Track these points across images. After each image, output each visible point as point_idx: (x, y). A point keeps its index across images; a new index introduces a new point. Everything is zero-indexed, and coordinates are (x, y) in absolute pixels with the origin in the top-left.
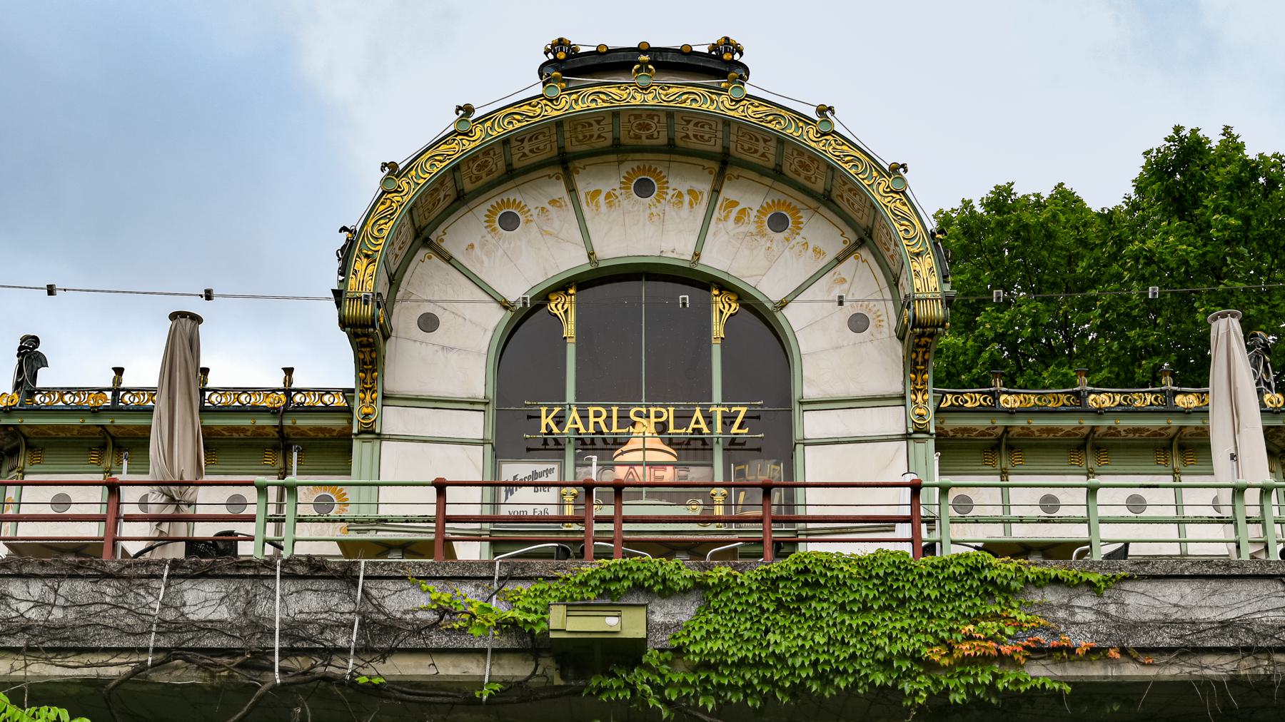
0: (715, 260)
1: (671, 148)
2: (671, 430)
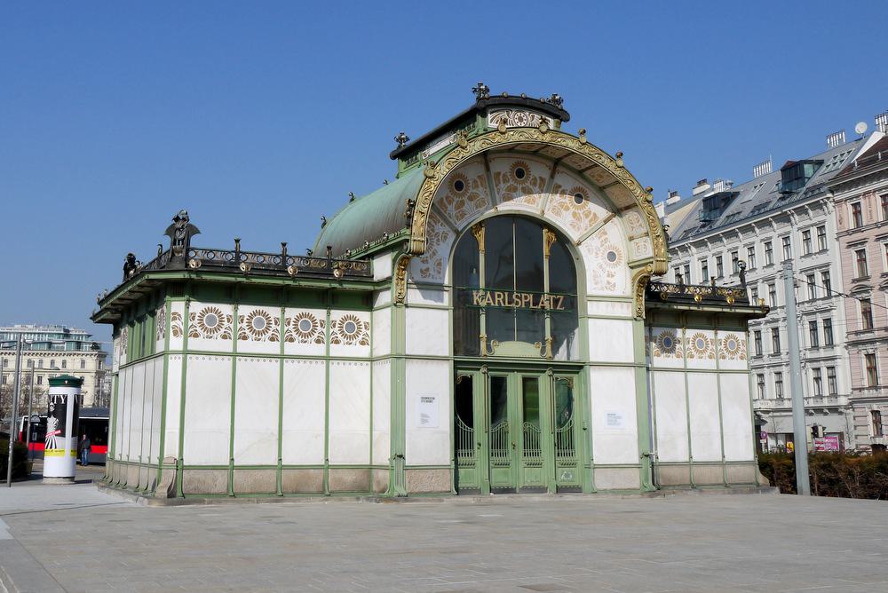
0: (550, 217)
1: (535, 153)
2: (531, 306)
